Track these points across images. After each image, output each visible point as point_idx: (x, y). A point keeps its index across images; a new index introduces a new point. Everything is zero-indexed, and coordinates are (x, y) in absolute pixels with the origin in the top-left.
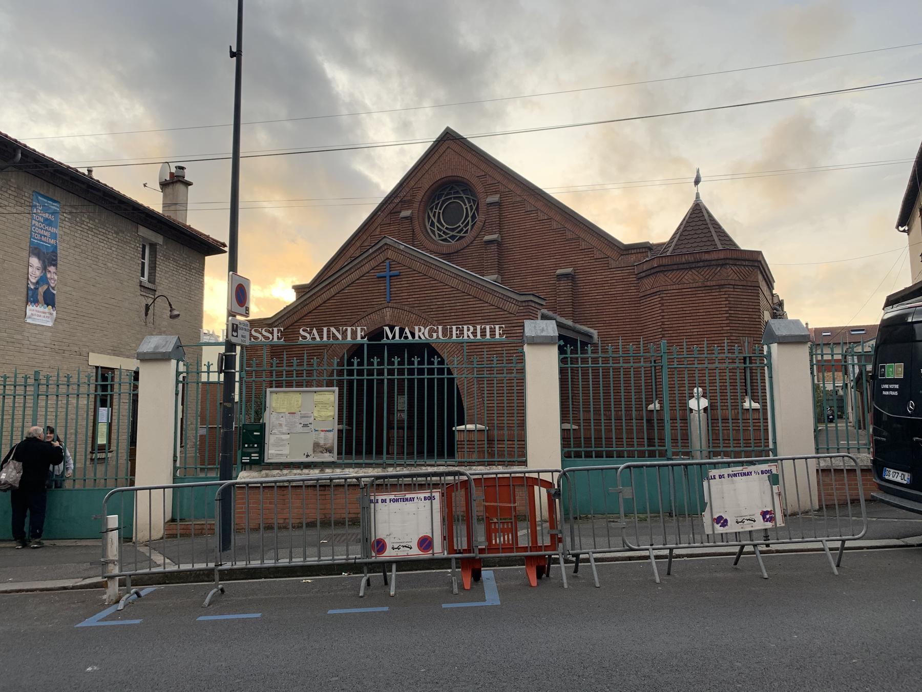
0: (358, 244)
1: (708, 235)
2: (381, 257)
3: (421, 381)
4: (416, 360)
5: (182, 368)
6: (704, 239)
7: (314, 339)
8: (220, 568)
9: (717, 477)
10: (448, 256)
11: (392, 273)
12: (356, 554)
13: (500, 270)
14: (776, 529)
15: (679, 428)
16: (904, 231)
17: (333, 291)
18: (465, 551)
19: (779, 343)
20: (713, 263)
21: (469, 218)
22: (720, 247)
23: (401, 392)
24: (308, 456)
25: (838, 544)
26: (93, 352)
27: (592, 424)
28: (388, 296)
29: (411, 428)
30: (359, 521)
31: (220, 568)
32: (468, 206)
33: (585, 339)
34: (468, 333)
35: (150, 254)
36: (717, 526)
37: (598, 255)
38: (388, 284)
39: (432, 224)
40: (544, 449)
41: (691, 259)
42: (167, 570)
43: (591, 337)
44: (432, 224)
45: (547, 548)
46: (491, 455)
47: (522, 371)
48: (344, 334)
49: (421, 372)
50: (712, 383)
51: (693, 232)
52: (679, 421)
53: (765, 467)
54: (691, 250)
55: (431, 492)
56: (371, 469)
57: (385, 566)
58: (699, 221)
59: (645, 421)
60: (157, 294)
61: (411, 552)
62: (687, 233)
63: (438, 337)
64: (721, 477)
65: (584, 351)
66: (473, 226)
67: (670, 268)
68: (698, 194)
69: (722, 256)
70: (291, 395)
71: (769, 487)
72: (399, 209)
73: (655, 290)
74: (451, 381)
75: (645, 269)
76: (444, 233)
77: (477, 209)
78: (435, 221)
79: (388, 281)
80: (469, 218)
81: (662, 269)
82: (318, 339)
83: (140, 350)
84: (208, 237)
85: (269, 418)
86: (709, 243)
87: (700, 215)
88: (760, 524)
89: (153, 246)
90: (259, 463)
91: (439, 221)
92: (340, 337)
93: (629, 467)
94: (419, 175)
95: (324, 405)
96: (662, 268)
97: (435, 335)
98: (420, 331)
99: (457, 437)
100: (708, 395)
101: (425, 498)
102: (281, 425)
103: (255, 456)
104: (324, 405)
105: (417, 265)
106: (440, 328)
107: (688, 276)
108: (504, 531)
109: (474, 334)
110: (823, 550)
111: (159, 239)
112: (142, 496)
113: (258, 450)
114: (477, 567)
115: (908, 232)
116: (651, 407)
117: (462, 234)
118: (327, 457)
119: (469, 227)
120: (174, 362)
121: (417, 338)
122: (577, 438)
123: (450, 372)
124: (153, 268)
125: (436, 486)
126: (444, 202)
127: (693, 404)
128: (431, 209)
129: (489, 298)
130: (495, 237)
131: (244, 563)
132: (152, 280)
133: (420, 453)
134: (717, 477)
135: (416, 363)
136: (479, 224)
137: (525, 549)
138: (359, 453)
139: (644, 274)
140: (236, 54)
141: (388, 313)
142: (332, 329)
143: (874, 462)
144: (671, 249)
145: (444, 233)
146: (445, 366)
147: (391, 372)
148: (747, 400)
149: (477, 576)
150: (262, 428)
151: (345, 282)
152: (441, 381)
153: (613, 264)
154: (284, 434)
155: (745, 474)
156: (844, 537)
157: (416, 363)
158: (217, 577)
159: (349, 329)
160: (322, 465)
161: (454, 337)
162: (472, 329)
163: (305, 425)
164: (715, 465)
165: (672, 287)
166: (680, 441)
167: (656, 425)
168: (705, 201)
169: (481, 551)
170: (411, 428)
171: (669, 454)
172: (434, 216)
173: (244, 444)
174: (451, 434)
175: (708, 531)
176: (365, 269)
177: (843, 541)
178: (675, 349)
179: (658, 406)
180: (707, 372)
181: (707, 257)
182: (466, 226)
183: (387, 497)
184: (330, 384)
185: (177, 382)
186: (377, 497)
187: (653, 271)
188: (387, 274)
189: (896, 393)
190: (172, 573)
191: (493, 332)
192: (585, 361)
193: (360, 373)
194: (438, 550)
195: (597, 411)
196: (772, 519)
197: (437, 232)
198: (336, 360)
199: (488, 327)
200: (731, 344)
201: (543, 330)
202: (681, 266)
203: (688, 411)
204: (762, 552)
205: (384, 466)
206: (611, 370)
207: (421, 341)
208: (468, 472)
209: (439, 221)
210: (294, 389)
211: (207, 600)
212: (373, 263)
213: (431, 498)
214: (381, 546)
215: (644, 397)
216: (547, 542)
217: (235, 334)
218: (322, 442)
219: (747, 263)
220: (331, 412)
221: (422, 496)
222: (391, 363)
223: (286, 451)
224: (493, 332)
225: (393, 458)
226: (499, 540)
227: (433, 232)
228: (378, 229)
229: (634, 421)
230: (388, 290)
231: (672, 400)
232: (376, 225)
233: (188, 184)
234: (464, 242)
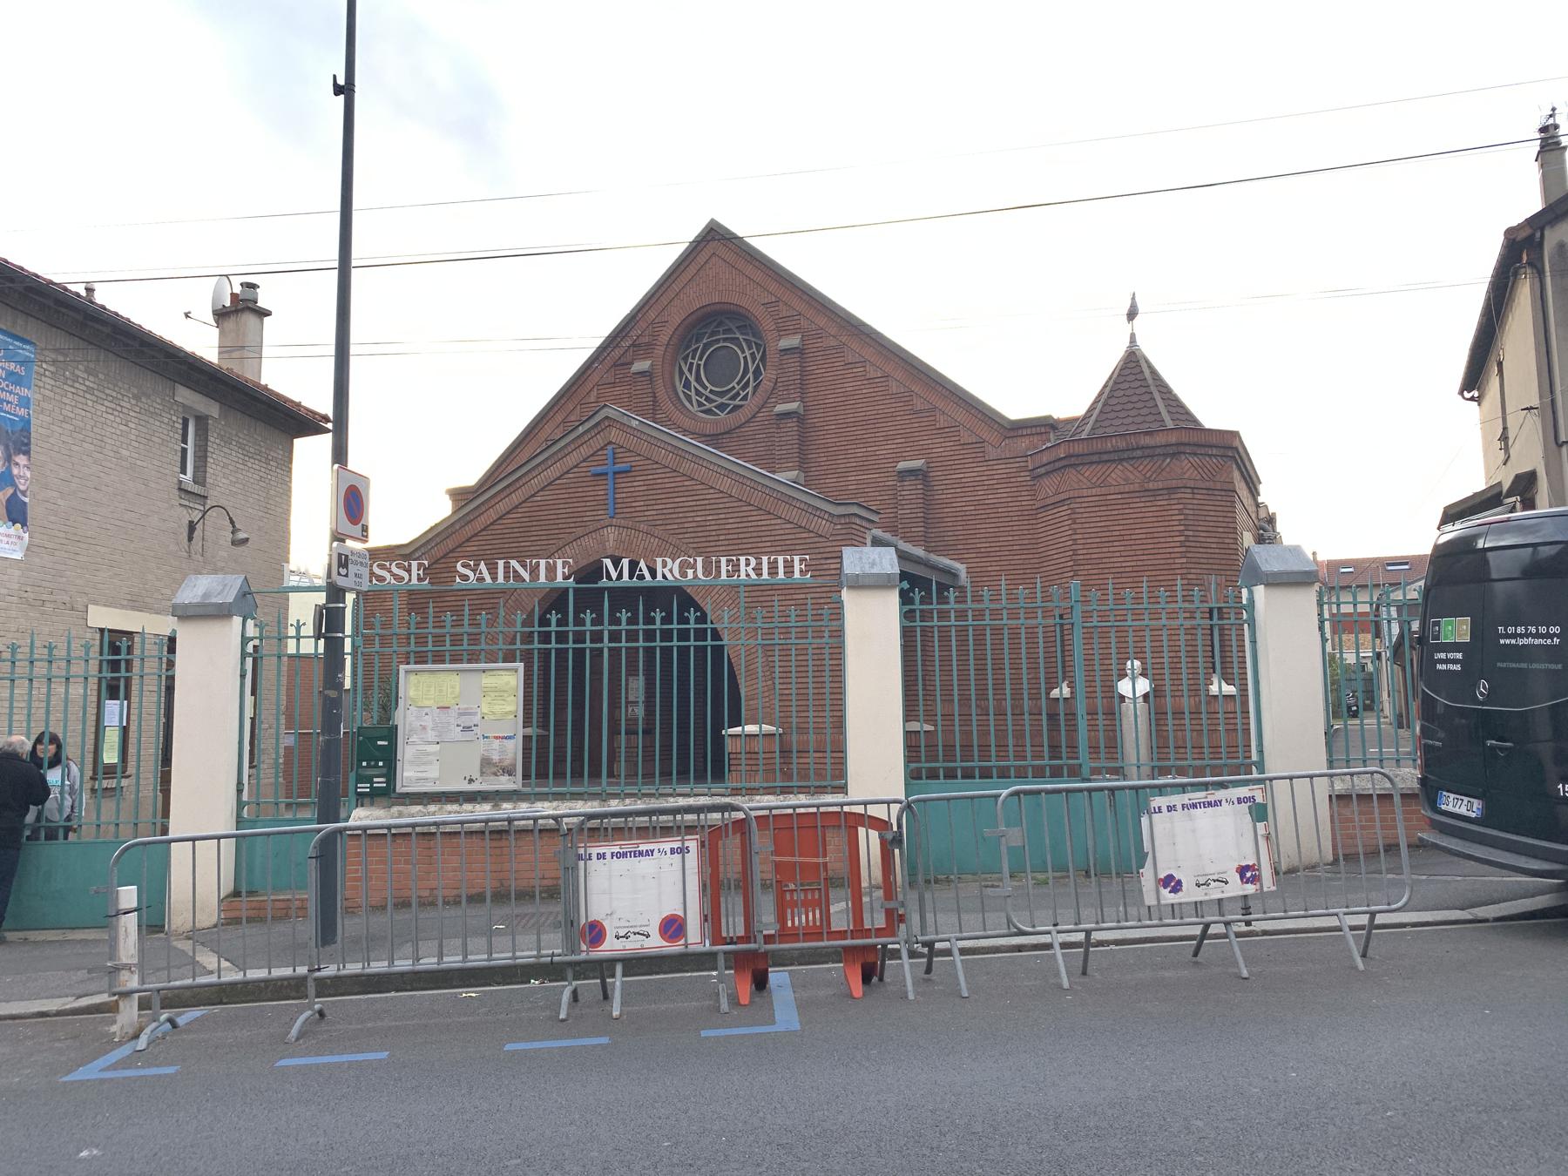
0: (559, 418)
1: (1151, 404)
2: (599, 441)
3: (667, 652)
4: (658, 615)
5: (251, 631)
7: (481, 580)
8: (317, 974)
9: (1164, 809)
10: (713, 439)
12: (553, 947)
13: (803, 464)
14: (1261, 895)
15: (1101, 728)
16: (1472, 399)
17: (515, 498)
18: (740, 940)
19: (1267, 585)
20: (1158, 451)
21: (750, 375)
22: (1170, 424)
23: (632, 671)
24: (471, 781)
25: (1364, 920)
26: (96, 603)
27: (957, 722)
29: (648, 732)
30: (559, 892)
32: (747, 353)
33: (945, 580)
34: (746, 571)
35: (196, 434)
36: (1165, 892)
37: (966, 437)
39: (687, 385)
40: (875, 764)
41: (1122, 444)
43: (955, 576)
44: (687, 385)
45: (879, 932)
46: (787, 776)
47: (839, 634)
48: (534, 571)
49: (667, 636)
50: (1157, 651)
51: (1125, 399)
52: (1100, 716)
53: (1243, 792)
54: (1122, 430)
55: (683, 841)
56: (580, 803)
57: (603, 968)
58: (1134, 381)
59: (1044, 717)
60: (209, 503)
61: (648, 943)
63: (696, 577)
64: (1170, 809)
65: (943, 600)
66: (756, 388)
67: (1087, 459)
68: (1133, 336)
69: (1174, 440)
70: (442, 676)
71: (1251, 826)
72: (629, 359)
73: (1062, 496)
74: (718, 651)
75: (1045, 460)
76: (707, 399)
77: (763, 359)
78: (692, 379)
79: (610, 482)
80: (750, 375)
81: (1073, 462)
82: (488, 580)
84: (299, 405)
85: (405, 718)
86: (1151, 418)
87: (1137, 370)
88: (1236, 888)
89: (202, 421)
90: (387, 795)
91: (698, 379)
92: (526, 576)
93: (1017, 793)
97: (690, 572)
98: (665, 565)
99: (729, 746)
100: (1150, 672)
101: (672, 851)
102: (424, 728)
103: (379, 782)
104: (500, 692)
106: (700, 560)
107: (1117, 474)
108: (806, 904)
109: (758, 570)
110: (1339, 929)
111: (213, 409)
112: (180, 853)
113: (384, 771)
114: (761, 966)
115: (1478, 400)
116: (1055, 693)
117: (737, 402)
118: (505, 783)
119: (750, 389)
120: (237, 620)
121: (659, 577)
122: (932, 747)
123: (716, 635)
125: (691, 829)
126: (706, 347)
127: (1124, 687)
128: (685, 359)
129: (783, 510)
130: (793, 406)
131: (360, 965)
132: (200, 479)
133: (666, 775)
134: (1164, 809)
136: (767, 385)
137: (842, 935)
138: (560, 775)
139: (1042, 470)
140: (345, 90)
141: (611, 535)
142: (513, 563)
143: (1423, 781)
144: (1089, 427)
145: (707, 399)
146: (709, 625)
147: (615, 637)
148: (1215, 680)
149: (761, 982)
151: (536, 483)
152: (701, 651)
153: (992, 453)
154: (430, 743)
155: (1210, 804)
156: (1373, 908)
158: (312, 990)
159: (543, 562)
161: (724, 576)
162: (753, 562)
163: (467, 729)
164: (1161, 790)
165: (1090, 492)
167: (1062, 723)
169: (769, 939)
170: (648, 732)
171: (1085, 771)
172: (690, 370)
173: (360, 761)
174: (719, 740)
175: (1150, 900)
176: (571, 460)
177: (1373, 914)
178: (1094, 594)
179: (1066, 691)
180: (1147, 633)
181: (1147, 441)
183: (608, 850)
184: (509, 657)
185: (244, 655)
186: (590, 850)
187: (1057, 465)
188: (610, 469)
189: (1458, 667)
190: (233, 985)
191: (789, 567)
192: (943, 615)
194: (695, 937)
195: (965, 700)
196: (1255, 879)
198: (520, 617)
199: (780, 559)
200: (1188, 587)
201: (873, 564)
202: (1105, 457)
203: (1116, 700)
204: (1238, 935)
205: (604, 797)
206: (988, 632)
207: (666, 584)
209: (698, 379)
210: (447, 666)
211: (294, 1032)
212: (585, 451)
213: (683, 851)
214: (596, 933)
215: (1042, 676)
216: (880, 922)
217: (343, 571)
218: (496, 757)
219: (1214, 451)
220: (512, 705)
221: (667, 847)
222: (615, 621)
223: (433, 772)
224: (789, 567)
225: (618, 784)
226: (799, 920)
227: (689, 398)
228: (595, 393)
229: (1026, 716)
230: (611, 496)
231: (1090, 682)
232: (589, 385)
234: (741, 416)
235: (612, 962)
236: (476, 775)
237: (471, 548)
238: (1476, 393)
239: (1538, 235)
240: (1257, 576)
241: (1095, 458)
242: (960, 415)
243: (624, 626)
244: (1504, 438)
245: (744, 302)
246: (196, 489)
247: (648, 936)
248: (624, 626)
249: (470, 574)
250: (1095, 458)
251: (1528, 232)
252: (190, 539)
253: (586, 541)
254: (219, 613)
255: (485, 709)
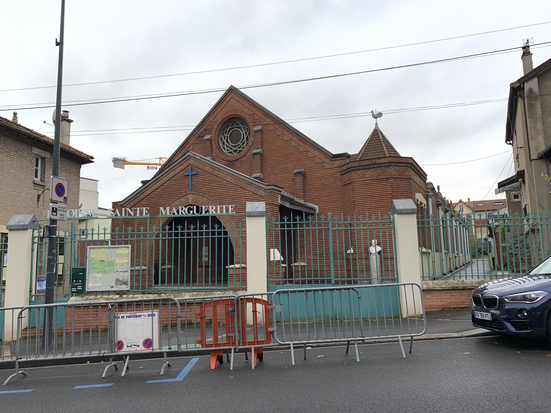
1: (381, 148)
4: (180, 227)
6: (379, 151)
7: (116, 215)
8: (19, 360)
10: (232, 163)
11: (194, 173)
15: (364, 264)
16: (510, 144)
17: (158, 184)
19: (398, 214)
20: (383, 165)
21: (245, 139)
22: (387, 155)
24: (112, 287)
28: (190, 187)
31: (19, 360)
32: (244, 132)
37: (318, 161)
38: (190, 180)
39: (223, 143)
40: (257, 282)
41: (370, 163)
42: (4, 361)
43: (315, 210)
44: (223, 143)
47: (245, 232)
49: (182, 234)
51: (373, 147)
54: (371, 157)
55: (152, 312)
57: (121, 358)
58: (377, 140)
59: (345, 260)
60: (46, 188)
61: (138, 349)
62: (369, 147)
63: (193, 213)
65: (307, 219)
68: (376, 124)
69: (388, 161)
74: (226, 239)
75: (344, 169)
76: (230, 148)
78: (225, 141)
79: (190, 178)
80: (245, 139)
82: (119, 215)
83: (9, 224)
86: (381, 153)
87: (377, 136)
89: (43, 159)
90: (81, 292)
91: (227, 141)
92: (132, 213)
94: (215, 114)
95: (122, 255)
96: (353, 169)
97: (191, 212)
98: (182, 209)
99: (229, 272)
101: (149, 315)
103: (80, 288)
104: (122, 255)
105: (207, 168)
107: (369, 173)
109: (216, 211)
111: (47, 155)
112: (8, 314)
115: (512, 144)
116: (349, 252)
117: (240, 149)
118: (124, 288)
119: (245, 145)
120: (30, 231)
123: (226, 233)
124: (43, 173)
126: (230, 130)
129: (249, 188)
130: (259, 150)
132: (42, 180)
135: (180, 229)
137: (211, 346)
139: (344, 172)
140: (60, 44)
141: (190, 197)
142: (128, 209)
144: (359, 157)
145: (230, 148)
146: (222, 230)
147: (164, 235)
150: (84, 270)
152: (219, 239)
153: (327, 166)
156: (412, 335)
157: (180, 229)
158: (17, 366)
159: (138, 209)
160: (121, 293)
166: (365, 272)
167: (351, 262)
168: (382, 128)
171: (333, 282)
172: (224, 138)
174: (226, 271)
176: (177, 171)
178: (336, 217)
179: (352, 251)
180: (368, 230)
181: (379, 161)
182: (243, 144)
183: (125, 315)
184: (126, 243)
185: (33, 243)
186: (118, 315)
187: (348, 170)
188: (190, 174)
193: (182, 234)
197: (226, 148)
199: (224, 206)
200: (383, 214)
202: (364, 167)
207: (182, 216)
208: (176, 299)
209: (227, 141)
210: (123, 246)
211: (6, 382)
212: (182, 167)
214: (120, 345)
215: (344, 245)
217: (55, 214)
218: (121, 279)
219: (403, 165)
220: (127, 260)
221: (147, 314)
227: (224, 148)
230: (190, 184)
232: (190, 144)
233: (71, 121)
234: (242, 154)
235: (126, 356)
236: (114, 285)
237: (143, 202)
238: (511, 142)
239: (522, 85)
240: (395, 211)
241: (361, 168)
242: (316, 153)
243: (204, 230)
244: (517, 158)
245: (243, 114)
246: (41, 183)
247: (139, 346)
248: (204, 230)
249: (113, 213)
250: (361, 168)
251: (519, 84)
252: (38, 201)
253: (181, 199)
254: (24, 228)
255: (117, 261)
